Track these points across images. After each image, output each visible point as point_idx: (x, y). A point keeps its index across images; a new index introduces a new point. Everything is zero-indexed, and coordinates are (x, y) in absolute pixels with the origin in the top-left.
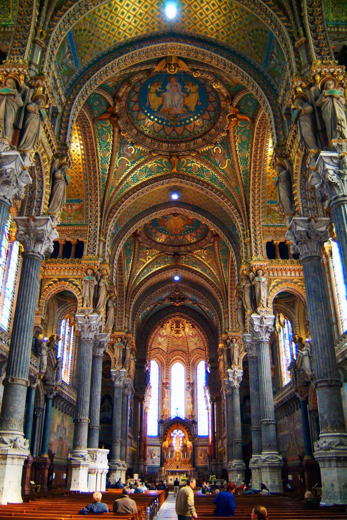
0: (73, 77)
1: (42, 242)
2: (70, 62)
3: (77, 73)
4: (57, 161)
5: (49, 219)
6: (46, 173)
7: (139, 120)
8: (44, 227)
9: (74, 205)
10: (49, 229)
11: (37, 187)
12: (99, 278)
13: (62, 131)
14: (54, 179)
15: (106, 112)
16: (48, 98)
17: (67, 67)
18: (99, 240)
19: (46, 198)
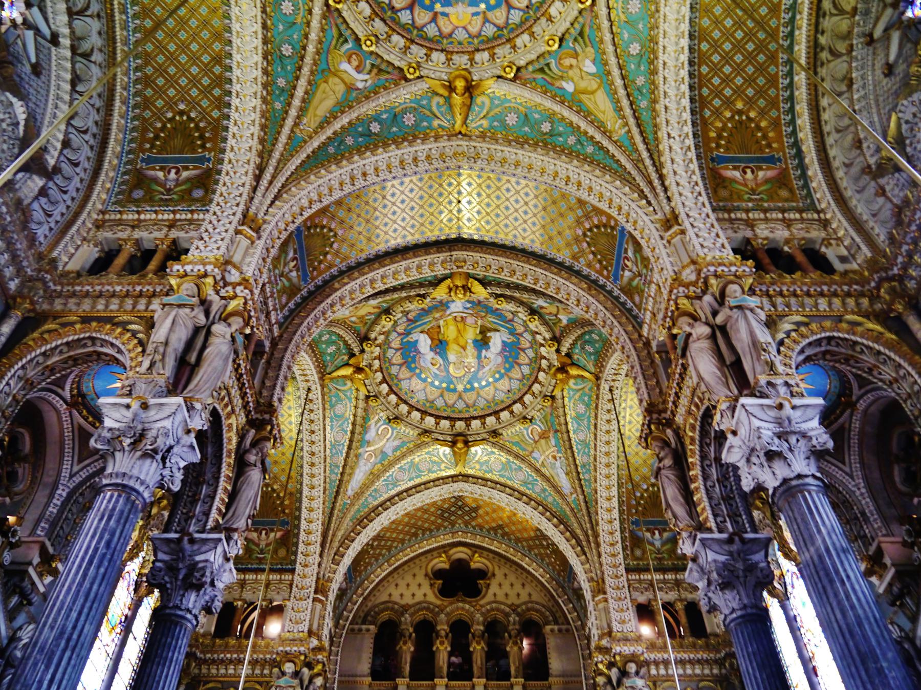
0: (298, 298)
1: (198, 587)
2: (294, 274)
3: (304, 292)
4: (253, 431)
5: (220, 540)
6: (229, 451)
7: (400, 380)
8: (211, 556)
9: (272, 530)
10: (220, 560)
11: (208, 476)
12: (306, 683)
13: (268, 383)
14: (241, 466)
15: (347, 365)
16: (250, 317)
17: (289, 280)
18: (314, 600)
19: (223, 500)
